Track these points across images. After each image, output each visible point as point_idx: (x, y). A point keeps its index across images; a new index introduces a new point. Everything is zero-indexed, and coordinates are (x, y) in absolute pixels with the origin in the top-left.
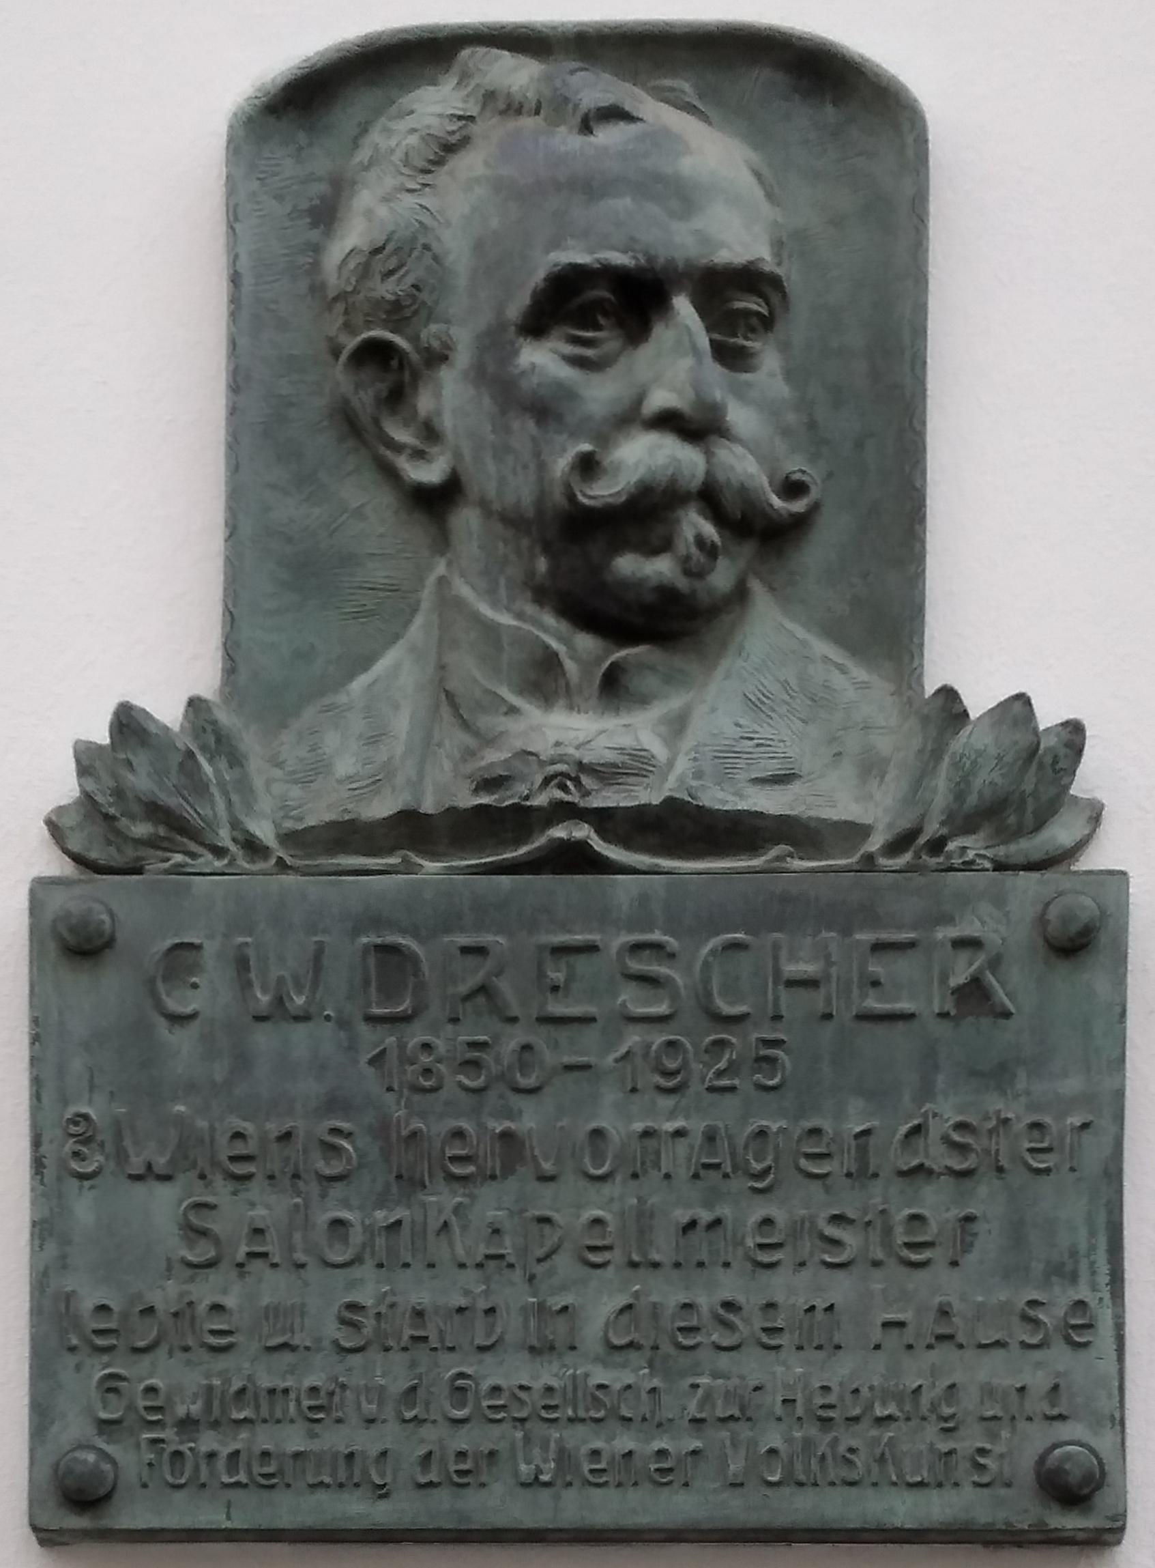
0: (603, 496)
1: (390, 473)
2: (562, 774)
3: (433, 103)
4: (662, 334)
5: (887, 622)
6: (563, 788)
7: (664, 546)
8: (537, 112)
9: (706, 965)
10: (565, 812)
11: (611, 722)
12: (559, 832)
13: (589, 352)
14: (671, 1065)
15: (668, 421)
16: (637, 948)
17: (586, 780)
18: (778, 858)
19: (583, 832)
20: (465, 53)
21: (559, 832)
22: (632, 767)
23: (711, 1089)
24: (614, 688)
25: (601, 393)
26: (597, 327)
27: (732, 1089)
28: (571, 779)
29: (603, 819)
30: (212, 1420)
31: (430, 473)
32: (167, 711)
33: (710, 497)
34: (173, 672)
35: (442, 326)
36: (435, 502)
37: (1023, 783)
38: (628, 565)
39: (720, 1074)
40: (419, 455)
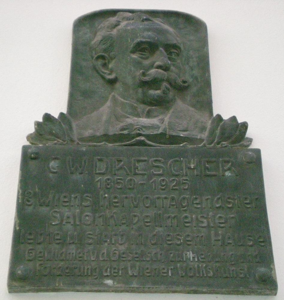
0: (146, 79)
1: (103, 78)
2: (139, 128)
3: (113, 20)
4: (158, 53)
5: (205, 103)
6: (139, 130)
7: (159, 89)
8: (133, 20)
9: (170, 165)
10: (140, 135)
11: (148, 120)
12: (138, 138)
13: (144, 56)
14: (164, 184)
15: (159, 67)
16: (156, 160)
17: (144, 129)
18: (185, 145)
19: (143, 138)
20: (119, 13)
21: (138, 138)
22: (153, 127)
23: (172, 189)
24: (149, 115)
25: (147, 62)
26: (145, 52)
27: (177, 189)
28: (140, 129)
29: (148, 137)
30: (68, 268)
31: (112, 77)
32: (56, 115)
33: (168, 81)
34: (58, 106)
35: (114, 53)
36: (112, 82)
37: (236, 131)
38: (152, 92)
39: (174, 186)
40: (109, 74)
